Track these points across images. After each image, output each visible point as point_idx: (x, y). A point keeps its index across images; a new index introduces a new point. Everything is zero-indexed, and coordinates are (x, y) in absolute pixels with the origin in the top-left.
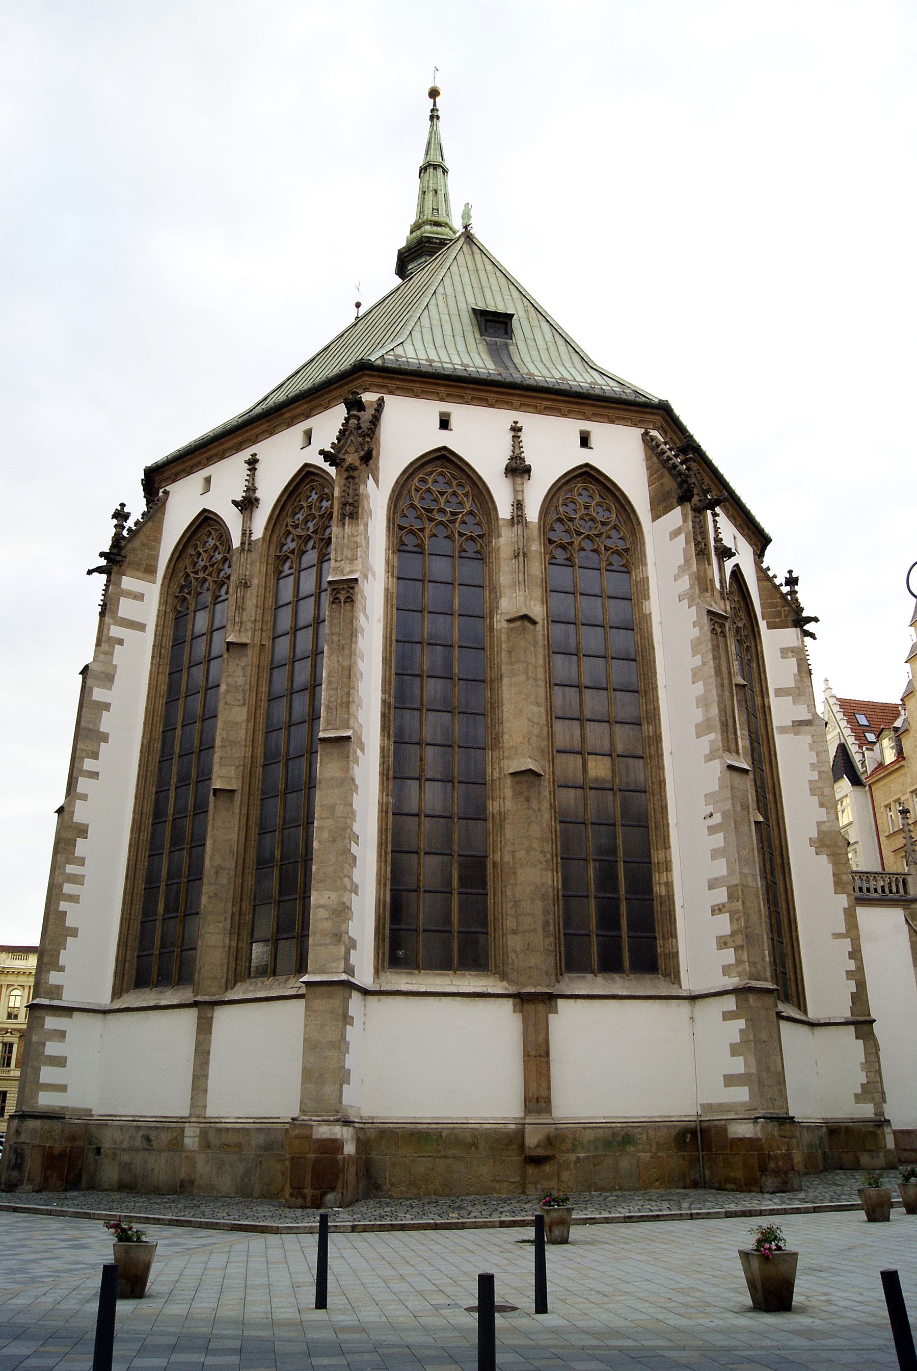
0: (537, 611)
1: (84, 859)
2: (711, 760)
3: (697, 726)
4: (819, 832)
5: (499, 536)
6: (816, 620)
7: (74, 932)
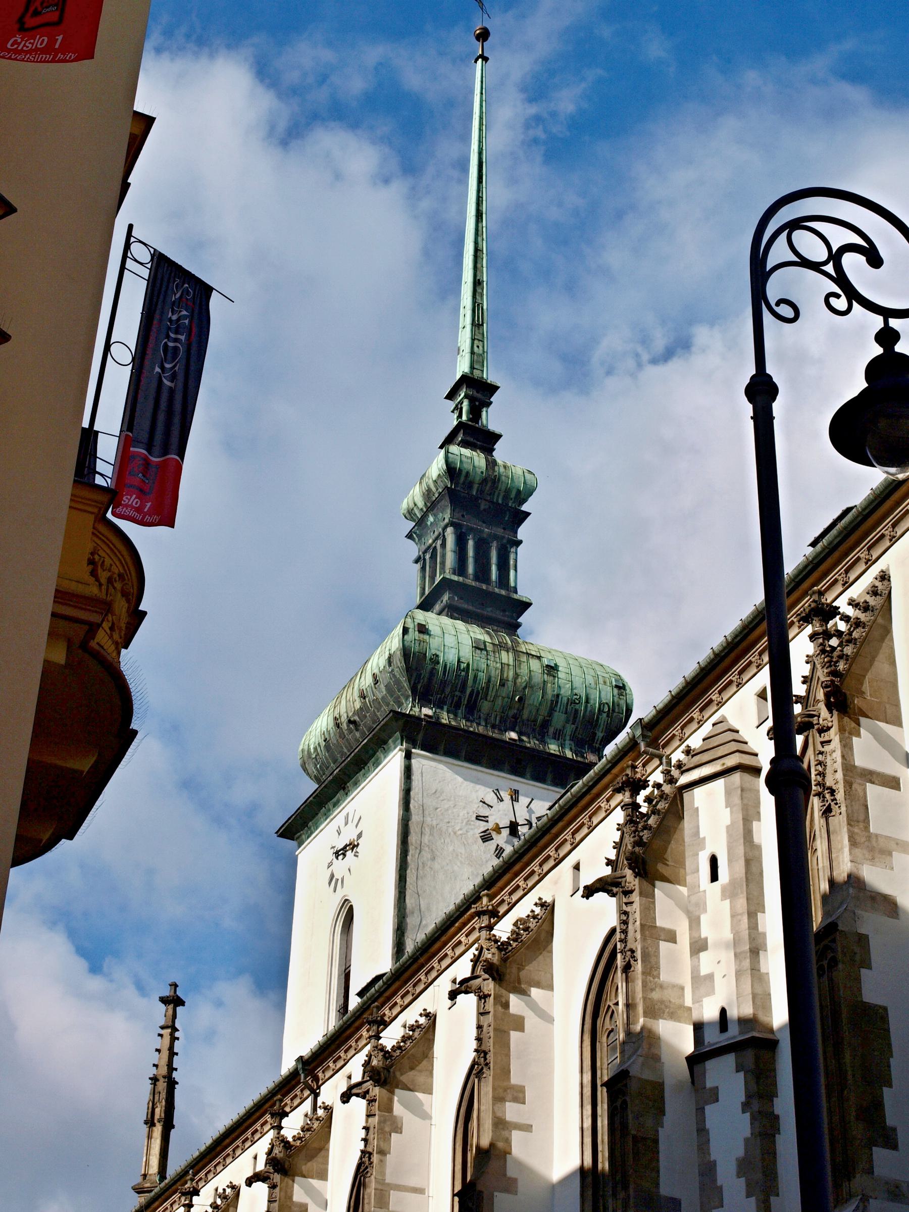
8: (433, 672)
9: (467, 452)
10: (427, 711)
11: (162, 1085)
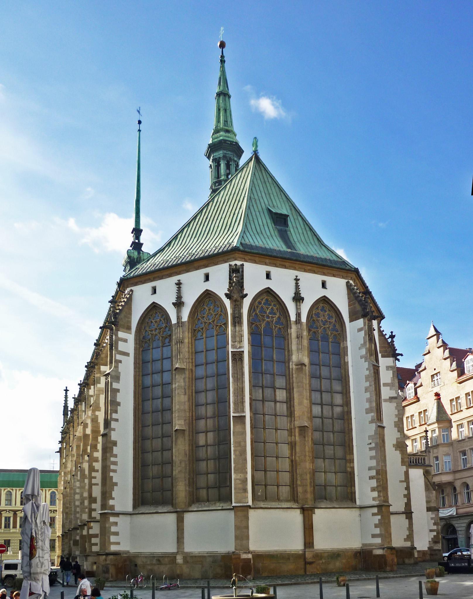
0: (306, 361)
1: (117, 455)
2: (372, 423)
3: (366, 409)
4: (397, 442)
5: (291, 328)
6: (402, 355)
7: (116, 484)
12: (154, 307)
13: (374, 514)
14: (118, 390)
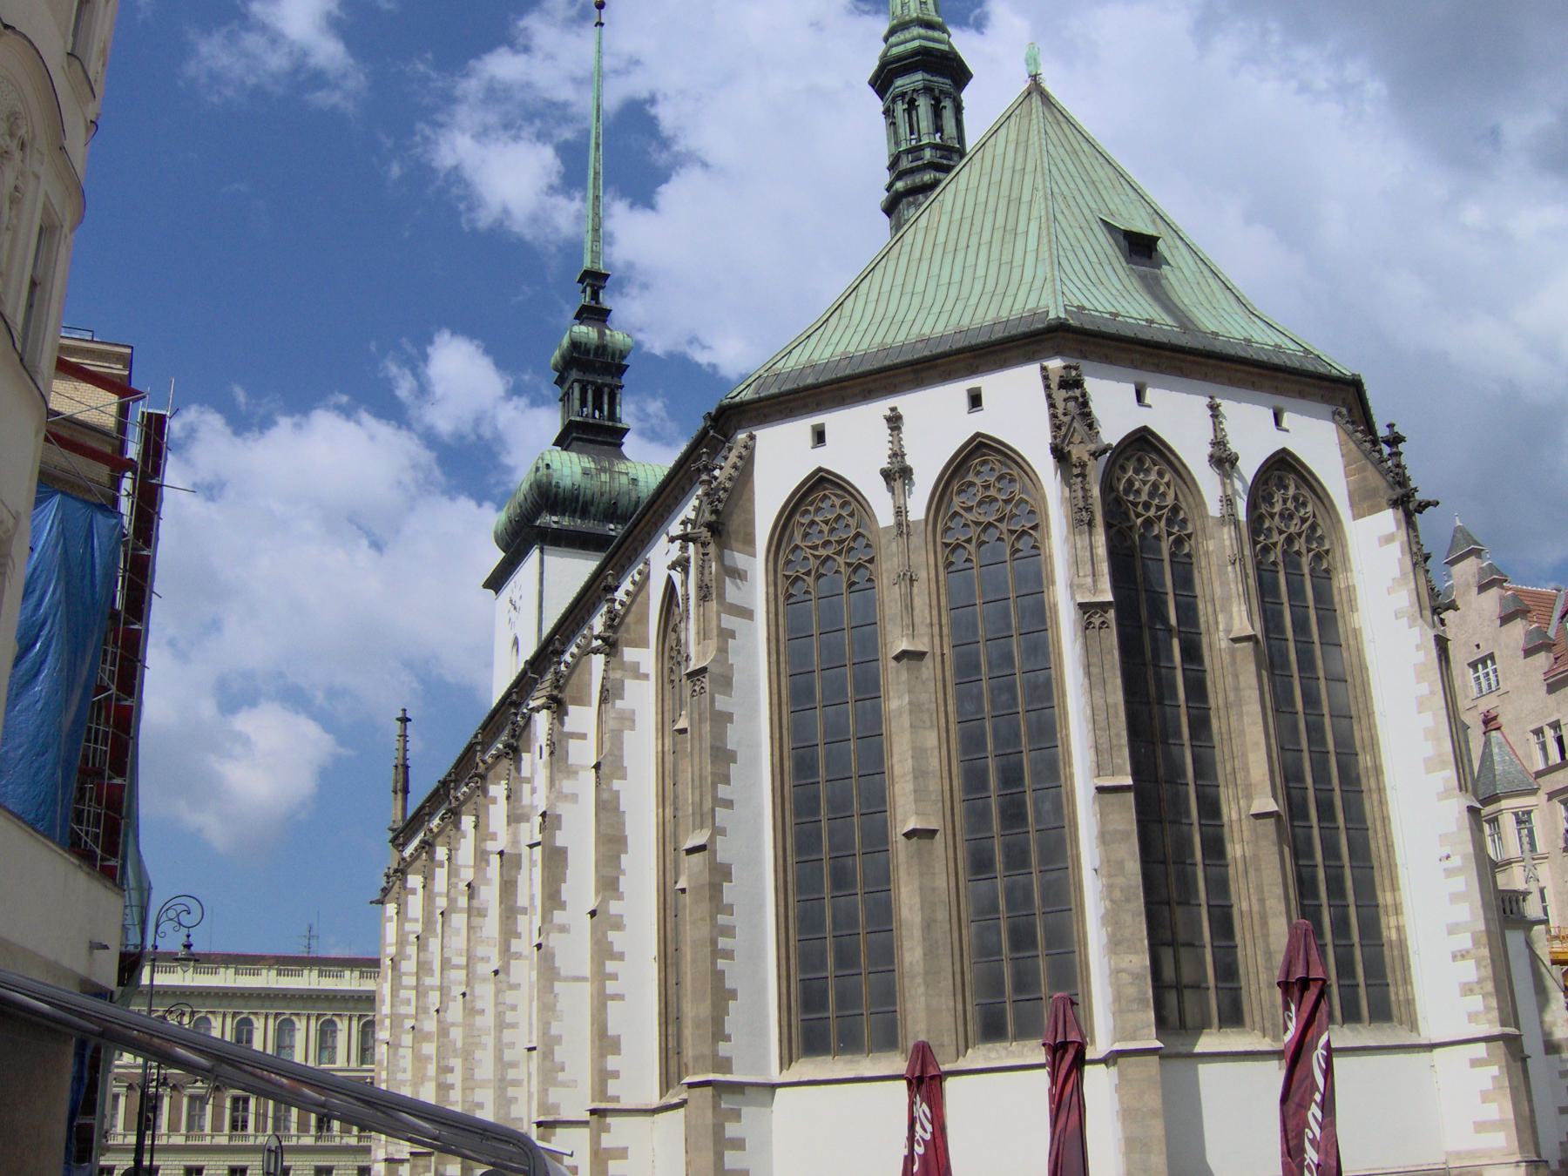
3: (1426, 760)
8: (556, 494)
9: (583, 329)
10: (555, 519)
11: (400, 769)
12: (821, 483)
13: (1475, 1063)
14: (728, 717)
